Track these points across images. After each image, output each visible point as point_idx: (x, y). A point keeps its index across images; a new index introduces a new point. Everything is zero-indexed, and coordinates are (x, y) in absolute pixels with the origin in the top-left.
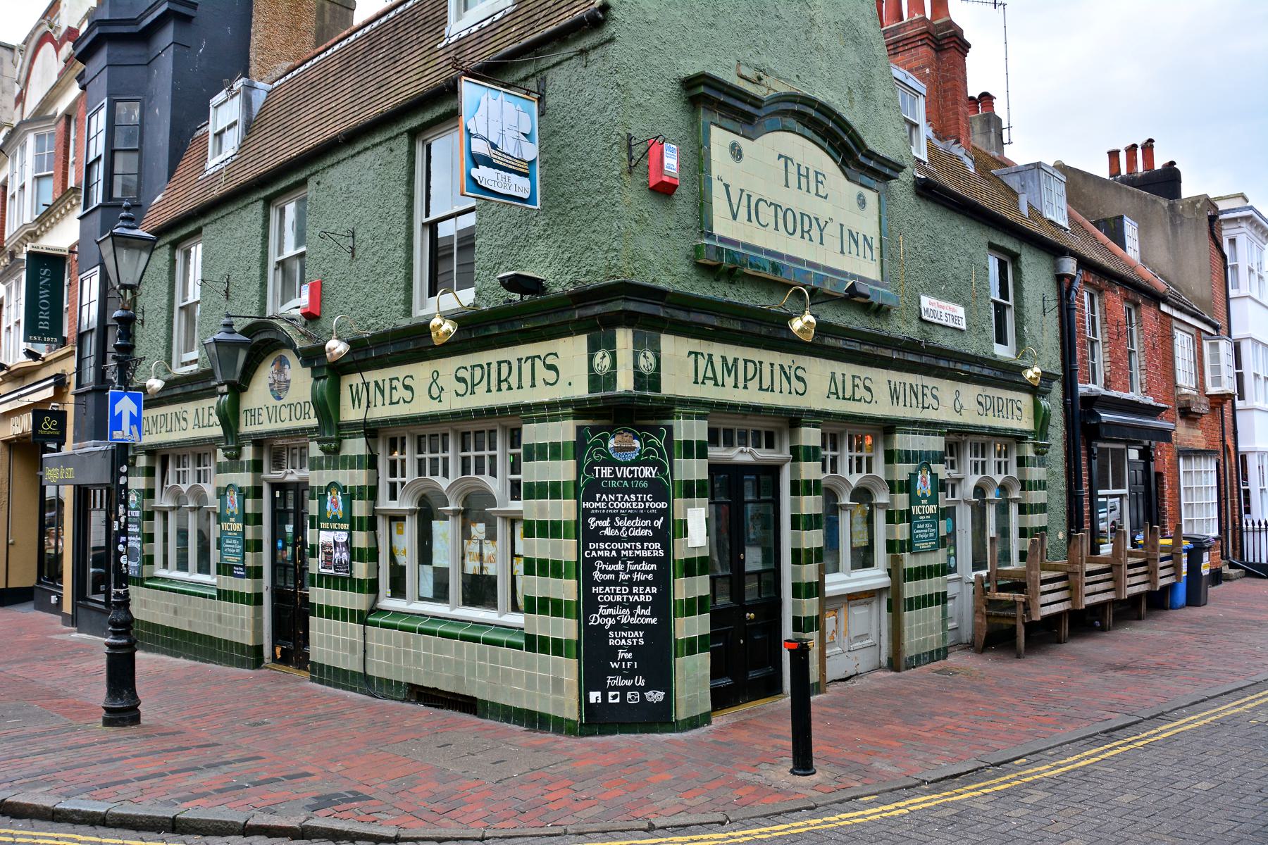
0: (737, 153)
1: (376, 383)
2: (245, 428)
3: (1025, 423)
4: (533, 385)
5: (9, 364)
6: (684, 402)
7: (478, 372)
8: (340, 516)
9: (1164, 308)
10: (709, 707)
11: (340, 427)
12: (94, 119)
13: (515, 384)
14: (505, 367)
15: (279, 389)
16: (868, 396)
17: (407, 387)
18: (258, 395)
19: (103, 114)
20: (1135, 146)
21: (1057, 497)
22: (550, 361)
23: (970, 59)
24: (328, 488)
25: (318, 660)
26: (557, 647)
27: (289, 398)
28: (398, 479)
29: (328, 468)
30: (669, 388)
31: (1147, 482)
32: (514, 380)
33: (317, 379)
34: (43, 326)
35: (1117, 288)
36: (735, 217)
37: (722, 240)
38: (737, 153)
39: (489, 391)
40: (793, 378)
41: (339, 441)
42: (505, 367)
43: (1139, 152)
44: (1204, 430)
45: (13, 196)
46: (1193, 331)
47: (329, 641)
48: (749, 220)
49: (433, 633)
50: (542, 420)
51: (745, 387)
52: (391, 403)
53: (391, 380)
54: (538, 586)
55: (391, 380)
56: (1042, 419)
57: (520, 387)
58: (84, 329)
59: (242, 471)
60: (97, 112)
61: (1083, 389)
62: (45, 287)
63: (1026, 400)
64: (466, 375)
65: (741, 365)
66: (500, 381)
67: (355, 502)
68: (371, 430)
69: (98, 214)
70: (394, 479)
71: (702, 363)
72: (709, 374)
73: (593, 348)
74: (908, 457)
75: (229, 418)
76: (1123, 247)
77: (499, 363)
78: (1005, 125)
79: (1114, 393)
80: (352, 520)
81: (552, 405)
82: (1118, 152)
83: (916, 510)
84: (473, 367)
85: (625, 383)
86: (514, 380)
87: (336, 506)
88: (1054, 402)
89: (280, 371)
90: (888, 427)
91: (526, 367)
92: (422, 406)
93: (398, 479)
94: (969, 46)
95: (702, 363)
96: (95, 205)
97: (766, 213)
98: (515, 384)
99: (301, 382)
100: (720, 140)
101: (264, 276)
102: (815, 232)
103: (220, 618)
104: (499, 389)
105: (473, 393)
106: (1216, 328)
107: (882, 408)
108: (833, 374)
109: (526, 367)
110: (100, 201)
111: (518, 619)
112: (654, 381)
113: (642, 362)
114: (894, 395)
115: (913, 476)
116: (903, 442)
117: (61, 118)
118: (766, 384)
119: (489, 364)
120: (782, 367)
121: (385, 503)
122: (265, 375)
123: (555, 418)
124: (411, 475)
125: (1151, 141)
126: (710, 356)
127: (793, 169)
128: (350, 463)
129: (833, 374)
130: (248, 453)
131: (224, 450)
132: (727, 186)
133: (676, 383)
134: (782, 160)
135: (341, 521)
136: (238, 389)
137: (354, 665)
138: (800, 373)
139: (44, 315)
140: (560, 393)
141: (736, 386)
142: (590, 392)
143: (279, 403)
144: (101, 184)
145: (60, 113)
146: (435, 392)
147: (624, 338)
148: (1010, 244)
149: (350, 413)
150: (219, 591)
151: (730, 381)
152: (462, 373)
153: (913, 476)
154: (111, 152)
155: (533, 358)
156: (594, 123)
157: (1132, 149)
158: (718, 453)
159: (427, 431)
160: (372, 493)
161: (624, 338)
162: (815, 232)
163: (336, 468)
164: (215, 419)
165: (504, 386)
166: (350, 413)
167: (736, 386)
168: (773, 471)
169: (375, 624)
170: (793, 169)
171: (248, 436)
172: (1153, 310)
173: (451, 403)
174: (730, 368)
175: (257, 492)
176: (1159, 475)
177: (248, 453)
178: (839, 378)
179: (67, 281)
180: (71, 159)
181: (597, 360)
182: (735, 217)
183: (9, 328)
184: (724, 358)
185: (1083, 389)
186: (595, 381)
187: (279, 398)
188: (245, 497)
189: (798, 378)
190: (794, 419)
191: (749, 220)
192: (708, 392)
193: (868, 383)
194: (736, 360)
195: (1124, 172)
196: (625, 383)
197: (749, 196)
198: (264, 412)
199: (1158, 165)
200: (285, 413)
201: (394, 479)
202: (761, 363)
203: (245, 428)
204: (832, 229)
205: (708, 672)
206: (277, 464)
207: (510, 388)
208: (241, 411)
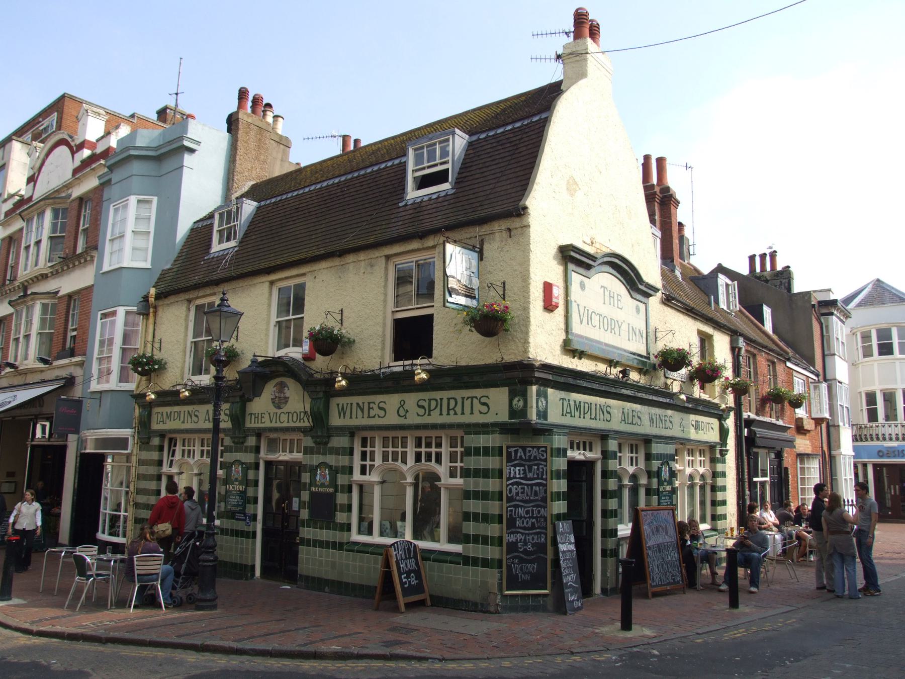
0: (583, 286)
1: (358, 404)
2: (250, 424)
3: (713, 436)
4: (472, 413)
7: (433, 404)
8: (327, 484)
9: (788, 364)
11: (328, 429)
14: (452, 403)
15: (280, 402)
20: (765, 254)
22: (483, 400)
24: (318, 466)
25: (305, 573)
26: (485, 563)
27: (289, 407)
28: (368, 463)
29: (318, 453)
31: (779, 474)
32: (459, 409)
36: (581, 322)
38: (583, 286)
39: (441, 414)
42: (452, 403)
43: (768, 258)
44: (811, 441)
45: (27, 248)
46: (804, 378)
47: (311, 561)
50: (476, 433)
52: (369, 417)
53: (369, 403)
55: (369, 403)
57: (463, 413)
59: (246, 451)
61: (745, 415)
63: (715, 422)
64: (426, 405)
65: (582, 405)
66: (449, 410)
67: (339, 476)
70: (364, 463)
71: (566, 403)
73: (512, 395)
74: (660, 457)
76: (762, 323)
77: (449, 399)
79: (761, 418)
80: (336, 487)
82: (755, 255)
83: (661, 488)
84: (430, 400)
85: (533, 416)
86: (459, 409)
87: (324, 477)
88: (730, 423)
90: (647, 440)
91: (467, 403)
92: (392, 419)
93: (368, 463)
97: (595, 318)
99: (298, 402)
100: (576, 278)
101: (267, 330)
102: (617, 329)
104: (448, 414)
105: (429, 415)
106: (817, 375)
107: (646, 428)
109: (467, 403)
111: (457, 548)
112: (543, 414)
114: (651, 420)
115: (660, 469)
116: (657, 448)
119: (441, 399)
121: (357, 476)
124: (378, 461)
125: (775, 252)
127: (607, 293)
128: (337, 451)
130: (251, 441)
131: (232, 438)
133: (554, 417)
135: (328, 487)
136: (245, 401)
143: (279, 411)
146: (402, 412)
149: (336, 420)
151: (577, 414)
152: (421, 403)
153: (660, 469)
155: (472, 398)
156: (516, 270)
157: (763, 257)
159: (394, 434)
160: (350, 470)
162: (617, 329)
163: (324, 454)
165: (452, 412)
166: (336, 420)
170: (607, 293)
171: (253, 429)
172: (782, 365)
173: (413, 419)
174: (578, 407)
175: (257, 466)
176: (786, 469)
178: (626, 411)
180: (81, 228)
181: (515, 402)
182: (581, 322)
183: (17, 340)
185: (745, 415)
186: (513, 413)
187: (280, 408)
188: (248, 469)
190: (604, 436)
199: (779, 268)
201: (364, 463)
203: (250, 424)
204: (624, 327)
206: (272, 448)
207: (456, 414)
208: (247, 413)
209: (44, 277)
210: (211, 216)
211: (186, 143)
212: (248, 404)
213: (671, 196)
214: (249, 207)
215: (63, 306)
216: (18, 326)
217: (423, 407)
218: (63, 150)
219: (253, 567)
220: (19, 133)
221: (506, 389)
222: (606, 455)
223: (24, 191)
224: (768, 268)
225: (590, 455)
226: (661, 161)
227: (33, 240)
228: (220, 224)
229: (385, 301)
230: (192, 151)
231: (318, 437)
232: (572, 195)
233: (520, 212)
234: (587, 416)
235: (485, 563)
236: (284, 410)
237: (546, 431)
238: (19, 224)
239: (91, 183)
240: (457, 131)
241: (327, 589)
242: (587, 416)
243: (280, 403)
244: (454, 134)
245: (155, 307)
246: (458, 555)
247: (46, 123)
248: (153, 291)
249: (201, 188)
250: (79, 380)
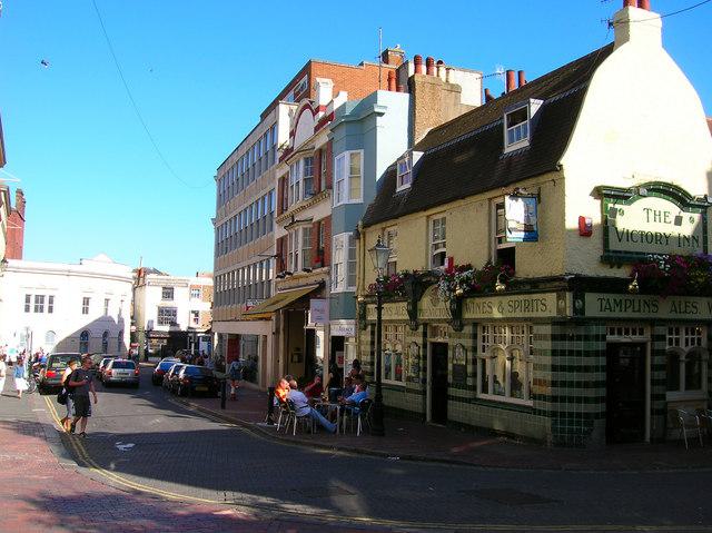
6: (595, 319)
15: (435, 302)
18: (425, 302)
26: (544, 413)
30: (589, 313)
37: (614, 252)
54: (538, 390)
68: (475, 324)
73: (559, 298)
75: (413, 313)
93: (486, 344)
112: (582, 311)
140: (547, 314)
145: (317, 147)
147: (569, 296)
151: (618, 309)
158: (610, 338)
160: (475, 349)
168: (643, 345)
170: (651, 215)
177: (421, 329)
186: (559, 311)
190: (652, 322)
196: (569, 313)
206: (434, 335)
209: (303, 208)
210: (395, 164)
211: (376, 110)
214: (417, 156)
215: (315, 230)
216: (291, 244)
218: (307, 111)
219: (425, 414)
220: (282, 96)
222: (656, 338)
225: (637, 338)
228: (401, 171)
229: (490, 230)
230: (381, 114)
233: (557, 169)
234: (630, 310)
235: (544, 413)
238: (287, 168)
239: (322, 140)
240: (532, 100)
241: (463, 430)
242: (630, 310)
244: (529, 103)
245: (364, 234)
246: (528, 407)
247: (302, 82)
248: (360, 223)
249: (392, 143)
250: (328, 283)
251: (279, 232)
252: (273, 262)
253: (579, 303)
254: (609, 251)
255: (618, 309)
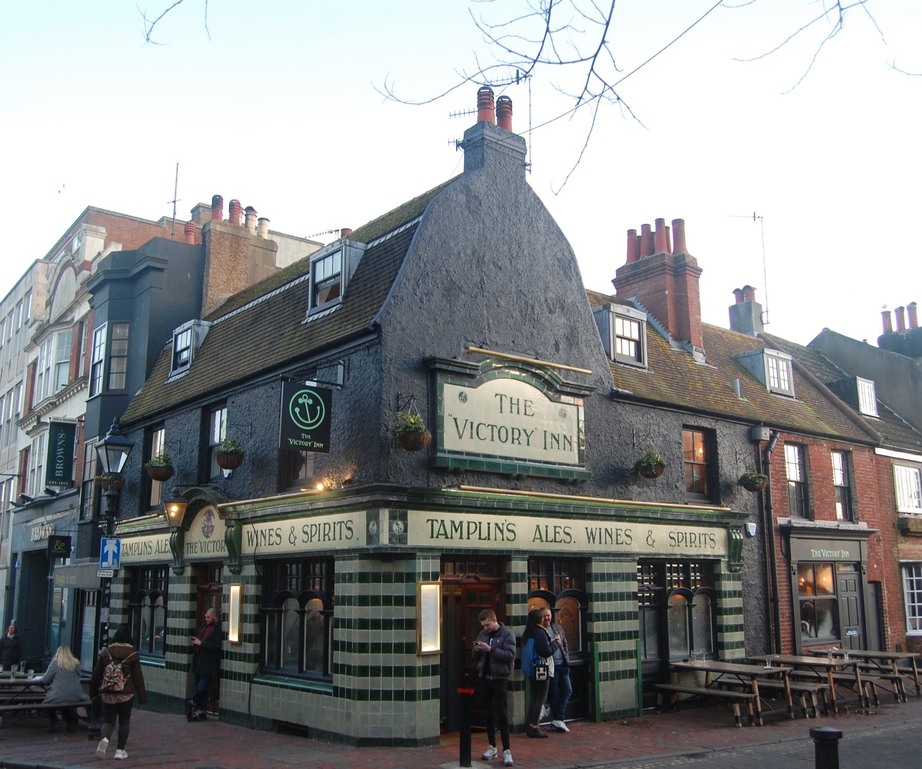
5: (33, 497)
6: (422, 549)
9: (879, 451)
10: (438, 732)
11: (240, 558)
12: (99, 334)
13: (332, 538)
14: (327, 526)
16: (567, 539)
17: (278, 535)
19: (105, 331)
20: (902, 308)
21: (754, 602)
23: (701, 280)
33: (229, 527)
34: (59, 474)
35: (823, 442)
36: (460, 437)
37: (450, 452)
38: (463, 397)
40: (505, 530)
41: (241, 566)
42: (327, 526)
43: (906, 313)
48: (472, 437)
49: (287, 687)
50: (344, 559)
51: (468, 538)
56: (734, 548)
57: (334, 539)
58: (87, 479)
60: (101, 329)
61: (782, 521)
62: (61, 446)
69: (100, 399)
72: (442, 531)
73: (369, 519)
78: (764, 309)
81: (349, 551)
85: (384, 540)
86: (331, 534)
89: (209, 520)
94: (701, 270)
95: (437, 526)
96: (97, 394)
97: (485, 432)
98: (332, 538)
102: (523, 438)
103: (166, 681)
108: (538, 526)
110: (100, 391)
112: (403, 538)
113: (395, 527)
117: (75, 324)
118: (484, 534)
120: (496, 524)
122: (199, 521)
123: (350, 559)
125: (914, 304)
126: (443, 521)
127: (506, 403)
129: (538, 526)
132: (455, 419)
134: (499, 397)
137: (243, 709)
138: (510, 527)
139: (59, 466)
141: (461, 538)
142: (367, 544)
143: (207, 540)
144: (101, 379)
147: (385, 514)
148: (705, 423)
150: (167, 663)
151: (456, 535)
154: (109, 357)
157: (900, 311)
161: (385, 514)
162: (523, 438)
164: (168, 547)
165: (327, 538)
167: (461, 538)
169: (256, 682)
170: (506, 403)
172: (866, 455)
179: (76, 441)
182: (460, 437)
183: (33, 470)
184: (453, 522)
187: (208, 537)
189: (509, 530)
191: (472, 437)
192: (442, 543)
193: (567, 530)
194: (461, 523)
195: (895, 328)
196: (384, 540)
197: (472, 423)
198: (198, 545)
200: (211, 546)
202: (480, 523)
205: (438, 711)
212: (186, 533)
213: (686, 265)
217: (306, 533)
221: (364, 513)
223: (45, 318)
224: (907, 326)
226: (678, 224)
227: (44, 370)
231: (233, 566)
232: (449, 301)
236: (211, 539)
237: (410, 555)
243: (208, 532)
251: (24, 441)
252: (14, 483)
253: (398, 527)
254: (444, 451)
255: (456, 535)
